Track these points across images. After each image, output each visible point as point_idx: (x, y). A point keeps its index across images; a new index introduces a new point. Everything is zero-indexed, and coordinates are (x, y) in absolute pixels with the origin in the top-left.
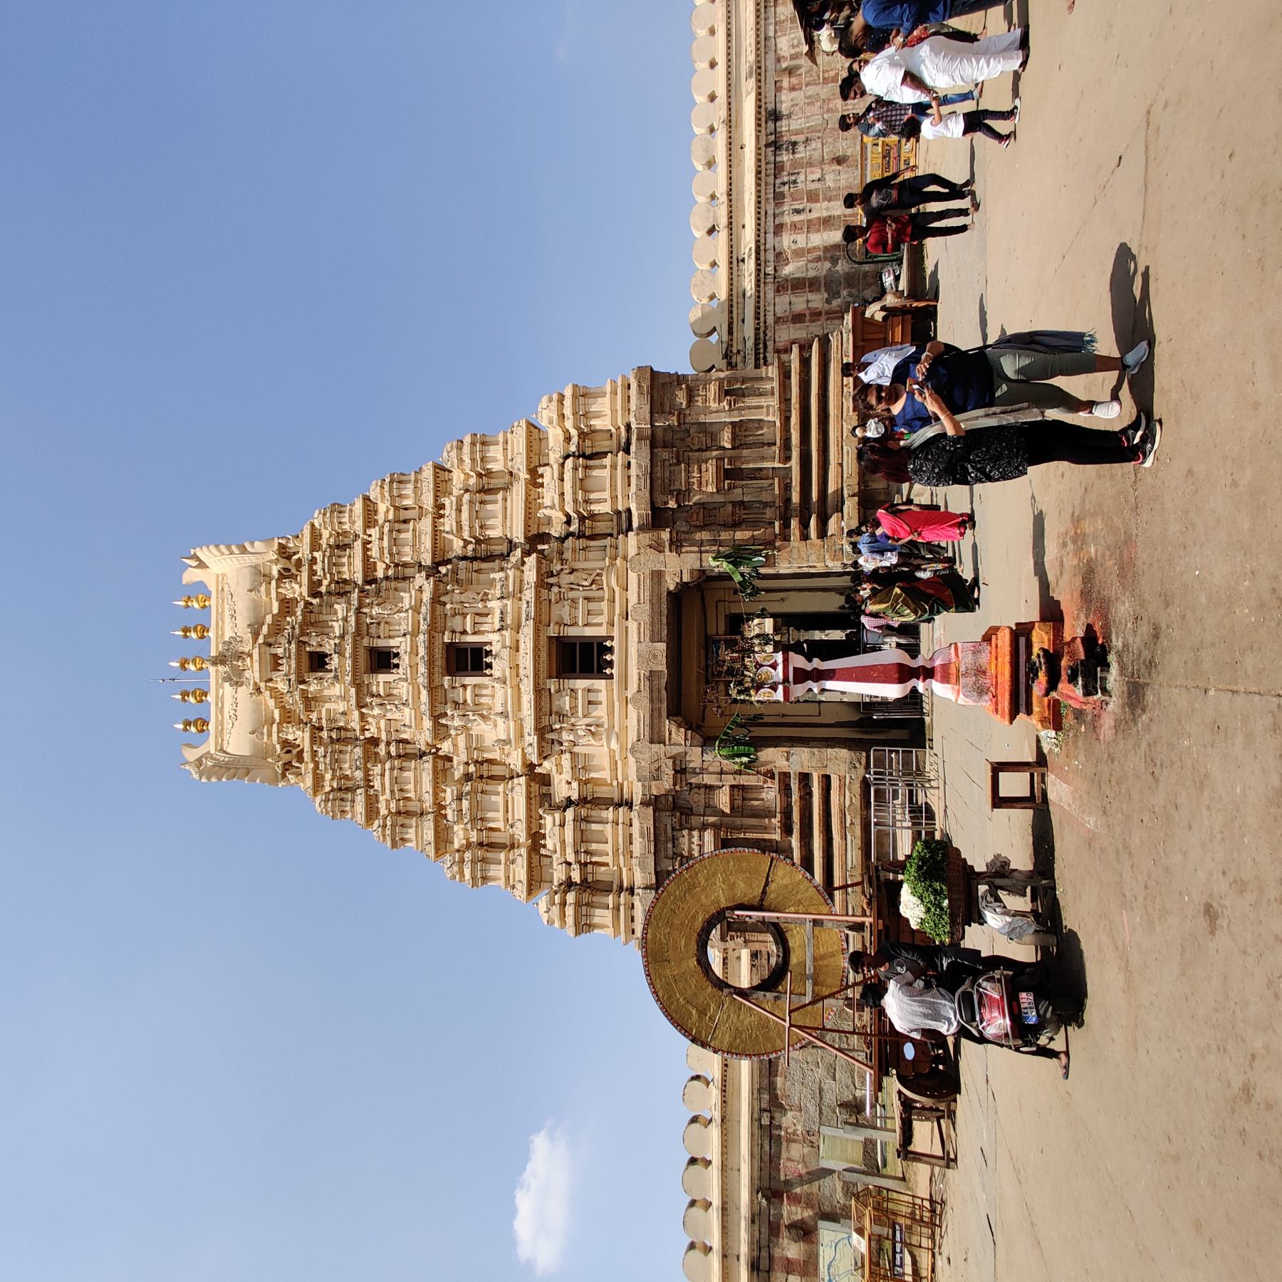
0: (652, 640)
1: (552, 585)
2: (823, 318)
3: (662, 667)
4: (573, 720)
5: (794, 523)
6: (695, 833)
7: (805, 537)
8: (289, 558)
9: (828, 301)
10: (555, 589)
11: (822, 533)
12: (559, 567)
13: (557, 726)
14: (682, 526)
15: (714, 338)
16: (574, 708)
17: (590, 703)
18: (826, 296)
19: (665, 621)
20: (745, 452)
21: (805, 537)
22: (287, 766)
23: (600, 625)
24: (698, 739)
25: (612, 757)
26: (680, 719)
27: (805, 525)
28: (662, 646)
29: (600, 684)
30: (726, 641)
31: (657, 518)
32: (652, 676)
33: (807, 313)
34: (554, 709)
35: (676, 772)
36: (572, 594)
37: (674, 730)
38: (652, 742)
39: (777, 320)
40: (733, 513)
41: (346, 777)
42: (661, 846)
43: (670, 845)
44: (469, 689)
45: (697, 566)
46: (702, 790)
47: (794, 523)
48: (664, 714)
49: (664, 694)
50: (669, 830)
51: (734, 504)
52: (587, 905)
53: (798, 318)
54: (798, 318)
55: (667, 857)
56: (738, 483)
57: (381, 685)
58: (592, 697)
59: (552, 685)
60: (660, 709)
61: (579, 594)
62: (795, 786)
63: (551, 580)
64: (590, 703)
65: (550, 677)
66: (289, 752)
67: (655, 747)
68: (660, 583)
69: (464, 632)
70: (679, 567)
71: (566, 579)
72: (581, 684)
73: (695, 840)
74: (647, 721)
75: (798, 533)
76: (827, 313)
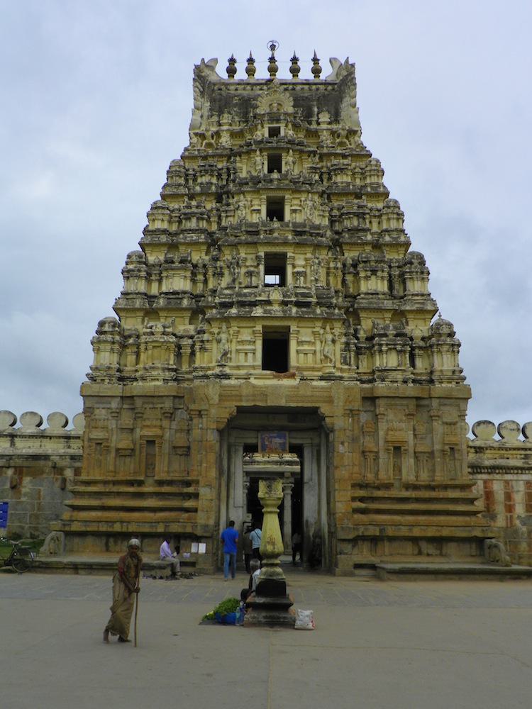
0: (287, 396)
1: (324, 329)
2: (509, 515)
3: (270, 403)
4: (234, 340)
5: (362, 493)
6: (158, 423)
7: (354, 499)
8: (347, 137)
9: (519, 517)
10: (322, 331)
11: (356, 511)
12: (337, 333)
13: (231, 332)
14: (364, 417)
15: (497, 437)
16: (242, 342)
17: (246, 354)
18: (523, 516)
19: (300, 405)
20: (412, 461)
21: (354, 499)
22: (202, 136)
23: (298, 362)
24: (222, 426)
25: (209, 368)
26: (235, 414)
27: (362, 499)
28: (283, 403)
29: (259, 362)
30: (284, 443)
31: (371, 399)
32: (263, 393)
33: (512, 503)
34: (242, 330)
35: (200, 411)
36: (318, 343)
37: (227, 410)
38: (220, 396)
39: (507, 482)
40: (370, 452)
41: (195, 180)
42: (151, 399)
43: (151, 406)
44: (256, 270)
45: (336, 427)
46: (186, 428)
47: (362, 493)
48: (238, 404)
49: (252, 404)
50: (162, 405)
51: (377, 453)
52: (112, 349)
53: (508, 497)
54: (508, 497)
55: (144, 403)
56: (392, 455)
57: (259, 208)
58: (250, 355)
59: (259, 328)
60: (241, 401)
61: (318, 347)
62: (191, 490)
63: (328, 328)
64: (246, 354)
65: (263, 327)
66: (212, 137)
67: (216, 398)
68: (325, 402)
69: (294, 266)
70: (336, 417)
71: (330, 337)
72: (259, 346)
73: (155, 423)
74: (233, 393)
75: (356, 495)
76: (511, 517)
